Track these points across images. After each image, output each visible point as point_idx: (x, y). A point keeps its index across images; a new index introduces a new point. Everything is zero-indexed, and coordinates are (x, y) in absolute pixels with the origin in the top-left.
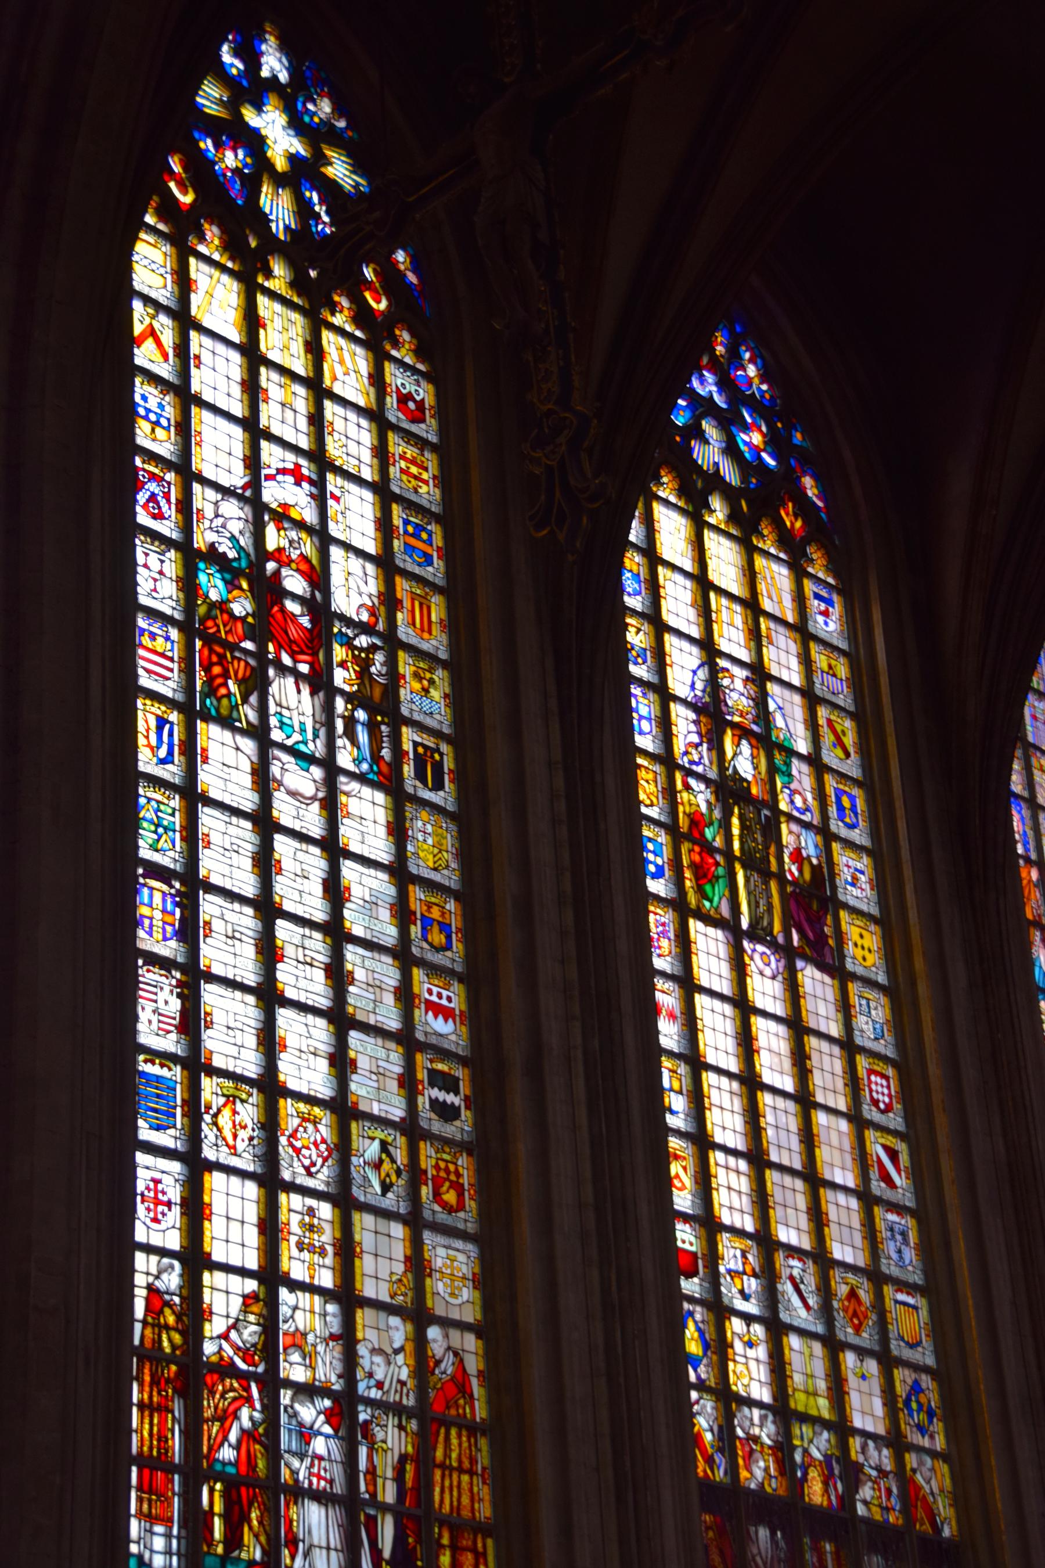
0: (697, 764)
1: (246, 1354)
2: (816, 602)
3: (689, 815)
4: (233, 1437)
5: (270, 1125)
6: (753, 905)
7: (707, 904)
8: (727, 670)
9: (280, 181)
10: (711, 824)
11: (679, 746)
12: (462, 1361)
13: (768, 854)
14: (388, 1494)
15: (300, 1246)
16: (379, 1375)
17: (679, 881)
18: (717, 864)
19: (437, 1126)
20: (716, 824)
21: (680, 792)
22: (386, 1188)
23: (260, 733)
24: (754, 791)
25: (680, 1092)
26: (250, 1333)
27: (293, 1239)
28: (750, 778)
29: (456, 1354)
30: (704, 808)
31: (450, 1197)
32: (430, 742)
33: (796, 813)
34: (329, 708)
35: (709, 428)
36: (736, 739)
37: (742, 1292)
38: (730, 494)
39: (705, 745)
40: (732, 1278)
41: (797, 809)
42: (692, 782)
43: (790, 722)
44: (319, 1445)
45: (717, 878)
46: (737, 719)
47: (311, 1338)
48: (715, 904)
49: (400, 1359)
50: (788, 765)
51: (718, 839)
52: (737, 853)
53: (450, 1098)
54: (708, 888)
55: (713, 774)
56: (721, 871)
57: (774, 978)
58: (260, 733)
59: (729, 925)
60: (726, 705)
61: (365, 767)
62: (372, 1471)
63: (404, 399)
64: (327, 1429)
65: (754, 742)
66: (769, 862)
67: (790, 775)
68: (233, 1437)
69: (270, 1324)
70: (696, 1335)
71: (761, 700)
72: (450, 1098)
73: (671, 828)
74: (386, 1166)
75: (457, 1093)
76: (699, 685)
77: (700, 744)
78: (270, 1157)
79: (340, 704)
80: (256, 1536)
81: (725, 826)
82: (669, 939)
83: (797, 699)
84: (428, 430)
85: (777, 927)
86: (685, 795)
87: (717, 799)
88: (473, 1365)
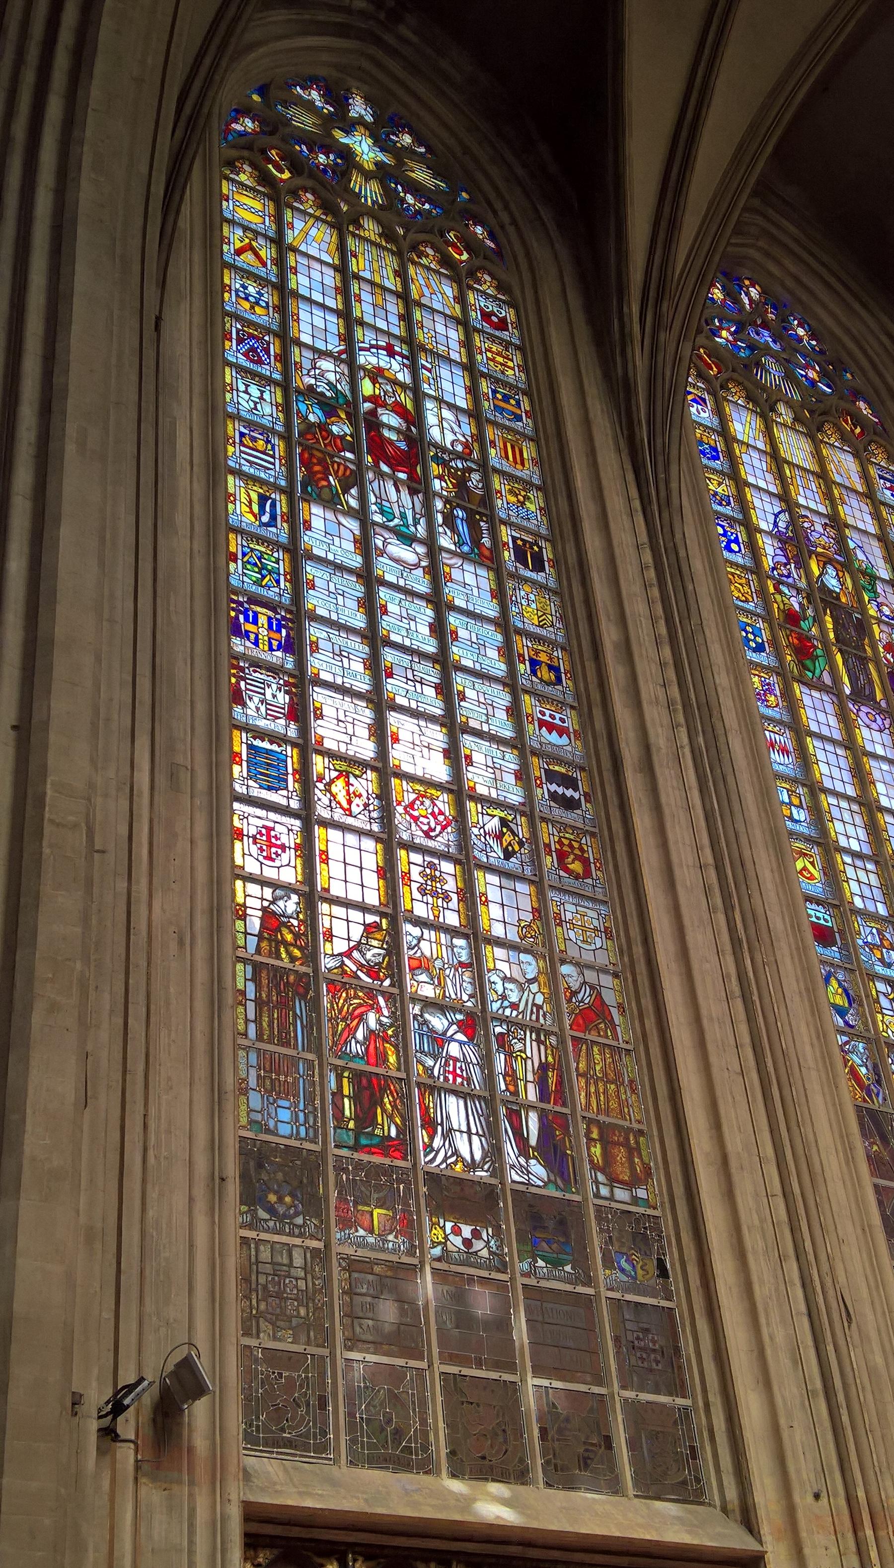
0: (788, 576)
1: (372, 971)
2: (882, 481)
3: (784, 611)
4: (360, 1035)
5: (384, 795)
6: (853, 680)
7: (810, 674)
8: (807, 517)
9: (368, 176)
10: (805, 619)
11: (768, 563)
12: (599, 994)
13: (863, 645)
14: (532, 1094)
15: (423, 891)
16: (514, 997)
17: (780, 657)
18: (816, 647)
19: (558, 812)
20: (811, 620)
21: (773, 594)
22: (508, 855)
23: (362, 515)
24: (843, 600)
25: (800, 806)
26: (374, 953)
27: (415, 886)
28: (838, 590)
29: (592, 988)
30: (797, 607)
31: (577, 867)
32: (529, 538)
33: (883, 618)
34: (428, 506)
35: (769, 362)
36: (821, 564)
37: (882, 960)
38: (789, 404)
39: (793, 565)
40: (871, 949)
41: (887, 616)
42: (785, 589)
43: (871, 558)
44: (454, 1049)
45: (817, 657)
46: (819, 550)
47: (438, 964)
48: (818, 672)
49: (534, 987)
50: (874, 586)
51: (813, 629)
52: (834, 640)
53: (569, 793)
54: (808, 663)
55: (803, 584)
56: (819, 652)
57: (881, 731)
58: (362, 515)
59: (834, 690)
60: (809, 540)
61: (466, 549)
62: (511, 1075)
63: (486, 316)
64: (460, 1037)
65: (839, 567)
66: (865, 650)
67: (875, 592)
68: (360, 1035)
69: (394, 947)
70: (840, 991)
71: (841, 541)
72: (569, 793)
73: (768, 618)
74: (508, 838)
75: (576, 789)
76: (782, 525)
77: (789, 563)
78: (387, 817)
79: (439, 504)
80: (391, 1117)
81: (818, 621)
82: (776, 696)
83: (875, 543)
84: (511, 335)
85: (879, 696)
86: (778, 597)
87: (809, 602)
88: (610, 998)
